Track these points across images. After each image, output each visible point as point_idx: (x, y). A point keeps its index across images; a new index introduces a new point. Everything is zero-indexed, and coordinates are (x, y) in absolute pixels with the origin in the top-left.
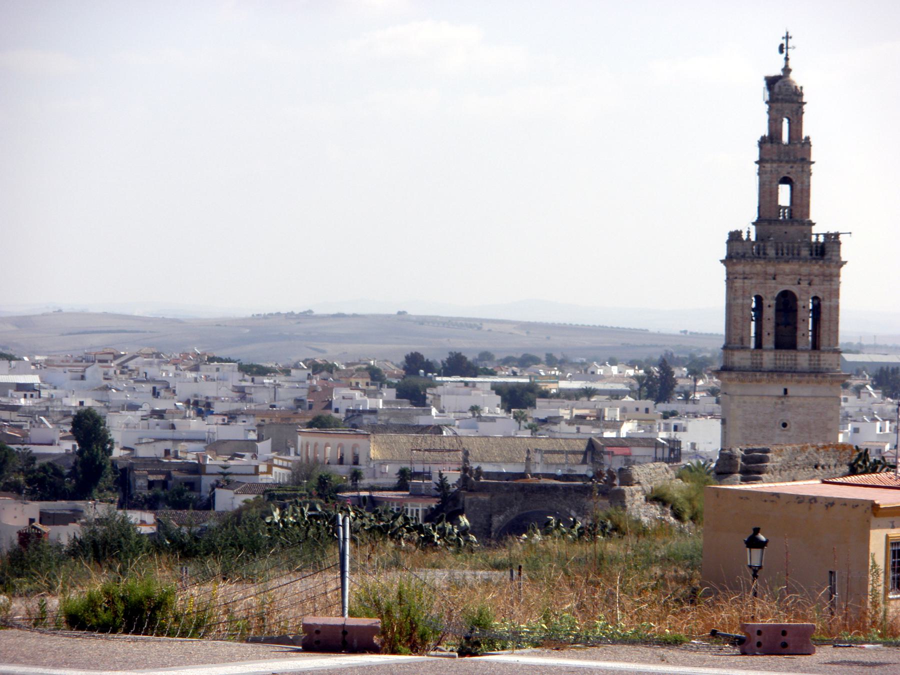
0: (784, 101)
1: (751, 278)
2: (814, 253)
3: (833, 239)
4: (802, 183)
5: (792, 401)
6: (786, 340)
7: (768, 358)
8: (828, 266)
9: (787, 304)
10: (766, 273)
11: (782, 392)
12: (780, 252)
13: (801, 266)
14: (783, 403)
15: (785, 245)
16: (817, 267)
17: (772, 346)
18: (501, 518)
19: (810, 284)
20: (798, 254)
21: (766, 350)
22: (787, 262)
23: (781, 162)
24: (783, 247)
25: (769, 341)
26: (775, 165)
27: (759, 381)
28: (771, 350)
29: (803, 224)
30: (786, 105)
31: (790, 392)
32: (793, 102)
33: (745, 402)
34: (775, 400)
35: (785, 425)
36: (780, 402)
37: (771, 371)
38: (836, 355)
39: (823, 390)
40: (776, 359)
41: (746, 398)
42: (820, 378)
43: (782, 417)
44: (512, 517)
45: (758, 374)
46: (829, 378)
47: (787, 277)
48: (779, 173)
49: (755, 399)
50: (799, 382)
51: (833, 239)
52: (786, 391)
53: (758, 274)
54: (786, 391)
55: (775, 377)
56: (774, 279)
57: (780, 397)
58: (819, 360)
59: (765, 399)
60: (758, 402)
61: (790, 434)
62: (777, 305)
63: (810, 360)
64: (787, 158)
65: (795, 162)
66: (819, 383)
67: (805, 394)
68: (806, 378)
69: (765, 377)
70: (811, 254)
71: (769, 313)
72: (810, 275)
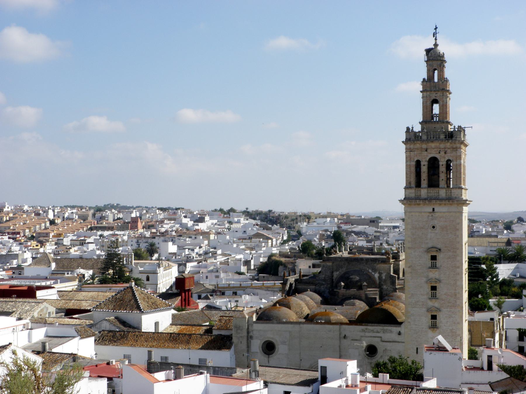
1: (414, 151)
2: (447, 137)
4: (443, 101)
5: (437, 214)
6: (433, 183)
7: (424, 192)
8: (455, 143)
9: (433, 163)
10: (422, 148)
11: (431, 210)
12: (429, 137)
13: (440, 144)
14: (432, 216)
15: (432, 133)
16: (449, 144)
17: (426, 186)
18: (338, 273)
19: (445, 153)
20: (439, 138)
21: (423, 188)
22: (432, 142)
23: (431, 91)
24: (430, 134)
25: (424, 183)
26: (428, 93)
27: (419, 204)
28: (425, 188)
29: (443, 122)
30: (434, 62)
31: (436, 210)
32: (438, 60)
33: (412, 216)
34: (428, 214)
35: (434, 227)
36: (430, 215)
37: (425, 199)
38: (460, 190)
40: (428, 193)
41: (413, 213)
42: (451, 202)
43: (432, 223)
44: (343, 273)
45: (418, 201)
46: (456, 202)
47: (433, 150)
48: (430, 97)
49: (417, 214)
50: (440, 205)
51: (461, 130)
52: (433, 209)
53: (418, 149)
54: (433, 209)
55: (427, 202)
56: (426, 151)
57: (430, 213)
58: (451, 193)
59: (423, 214)
60: (419, 216)
61: (436, 232)
62: (428, 164)
63: (446, 193)
64: (435, 89)
65: (438, 91)
66: (451, 204)
67: (444, 211)
68: (444, 202)
69: (421, 202)
70: (446, 138)
71: (424, 169)
72: (445, 148)
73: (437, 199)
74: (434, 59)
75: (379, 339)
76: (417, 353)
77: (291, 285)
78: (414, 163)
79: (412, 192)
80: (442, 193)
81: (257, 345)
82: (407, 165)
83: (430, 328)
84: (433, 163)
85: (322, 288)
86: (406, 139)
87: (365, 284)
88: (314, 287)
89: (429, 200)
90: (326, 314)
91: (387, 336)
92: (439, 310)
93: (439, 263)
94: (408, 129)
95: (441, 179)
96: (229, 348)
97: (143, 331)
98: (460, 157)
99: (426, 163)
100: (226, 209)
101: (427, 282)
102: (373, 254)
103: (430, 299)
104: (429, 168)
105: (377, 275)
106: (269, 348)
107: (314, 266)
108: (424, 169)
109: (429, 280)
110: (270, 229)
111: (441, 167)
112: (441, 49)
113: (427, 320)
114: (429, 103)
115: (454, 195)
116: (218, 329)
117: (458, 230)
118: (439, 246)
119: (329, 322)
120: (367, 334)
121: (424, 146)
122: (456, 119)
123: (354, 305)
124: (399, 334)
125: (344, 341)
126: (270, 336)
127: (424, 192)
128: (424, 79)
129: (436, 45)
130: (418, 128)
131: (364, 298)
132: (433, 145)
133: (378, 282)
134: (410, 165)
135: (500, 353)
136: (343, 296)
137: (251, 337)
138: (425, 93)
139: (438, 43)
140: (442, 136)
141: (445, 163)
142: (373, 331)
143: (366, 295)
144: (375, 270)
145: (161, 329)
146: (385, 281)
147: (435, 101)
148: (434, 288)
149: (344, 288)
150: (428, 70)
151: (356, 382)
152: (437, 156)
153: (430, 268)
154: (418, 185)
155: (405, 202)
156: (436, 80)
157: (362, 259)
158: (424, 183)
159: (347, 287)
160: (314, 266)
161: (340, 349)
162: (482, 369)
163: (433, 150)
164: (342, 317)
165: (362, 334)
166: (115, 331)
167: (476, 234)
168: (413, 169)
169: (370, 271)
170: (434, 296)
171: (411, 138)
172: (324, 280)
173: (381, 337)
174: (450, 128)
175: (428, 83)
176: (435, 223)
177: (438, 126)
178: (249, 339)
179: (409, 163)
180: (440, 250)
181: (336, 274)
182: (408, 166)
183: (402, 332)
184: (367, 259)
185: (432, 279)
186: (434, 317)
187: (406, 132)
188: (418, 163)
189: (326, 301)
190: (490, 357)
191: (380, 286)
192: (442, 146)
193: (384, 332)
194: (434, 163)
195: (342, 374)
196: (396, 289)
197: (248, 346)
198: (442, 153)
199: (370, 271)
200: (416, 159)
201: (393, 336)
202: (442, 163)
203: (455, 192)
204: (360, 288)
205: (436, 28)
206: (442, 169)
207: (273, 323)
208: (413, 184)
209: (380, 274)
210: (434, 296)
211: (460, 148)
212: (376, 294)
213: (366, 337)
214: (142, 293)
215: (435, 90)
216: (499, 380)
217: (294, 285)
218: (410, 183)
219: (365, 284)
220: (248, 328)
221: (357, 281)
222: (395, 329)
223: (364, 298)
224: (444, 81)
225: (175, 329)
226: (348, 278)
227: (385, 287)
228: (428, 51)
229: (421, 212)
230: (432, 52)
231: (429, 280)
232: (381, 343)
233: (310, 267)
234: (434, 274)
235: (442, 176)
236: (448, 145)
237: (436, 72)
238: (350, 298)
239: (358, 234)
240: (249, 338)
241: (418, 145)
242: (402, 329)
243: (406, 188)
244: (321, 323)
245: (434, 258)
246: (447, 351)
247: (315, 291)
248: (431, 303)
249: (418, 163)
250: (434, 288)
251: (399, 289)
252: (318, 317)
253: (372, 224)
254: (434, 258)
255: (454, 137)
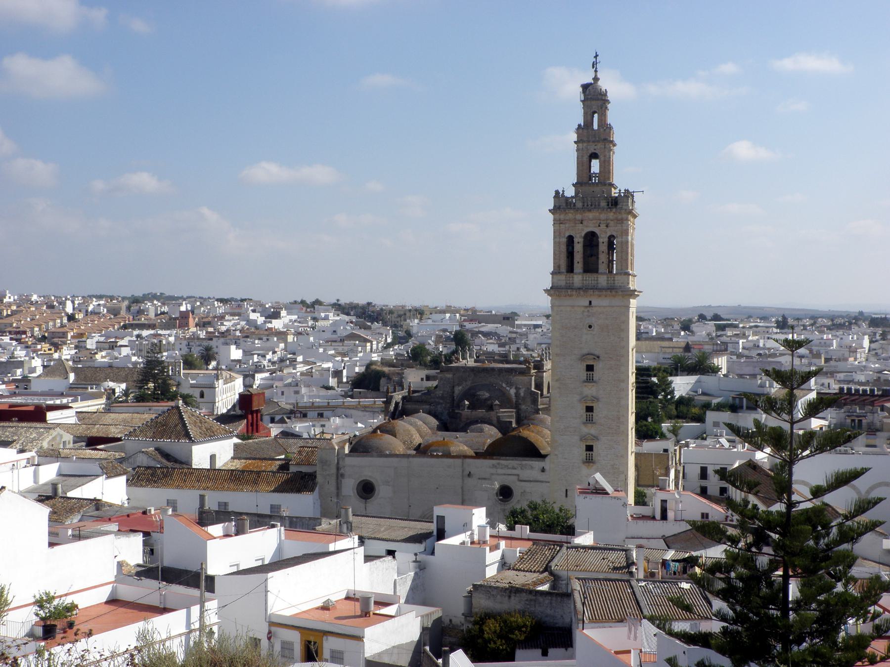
0: (592, 99)
3: (628, 195)
5: (595, 309)
6: (590, 267)
7: (578, 279)
9: (591, 239)
13: (600, 213)
17: (581, 271)
22: (590, 211)
23: (589, 142)
25: (578, 267)
26: (585, 144)
27: (571, 296)
28: (579, 274)
29: (605, 184)
30: (594, 102)
32: (598, 100)
34: (583, 309)
35: (590, 327)
37: (579, 289)
39: (617, 301)
47: (591, 222)
50: (600, 296)
51: (628, 195)
52: (590, 302)
53: (570, 220)
54: (590, 302)
57: (586, 307)
62: (584, 242)
65: (598, 142)
66: (614, 296)
71: (578, 248)
73: (595, 288)
74: (594, 98)
75: (515, 478)
76: (566, 496)
77: (397, 404)
78: (564, 240)
79: (562, 279)
80: (602, 280)
81: (349, 486)
82: (555, 243)
83: (584, 463)
84: (591, 239)
85: (439, 409)
86: (555, 206)
87: (497, 402)
88: (428, 407)
89: (584, 289)
90: (443, 443)
91: (526, 474)
92: (596, 438)
93: (597, 374)
94: (557, 192)
95: (600, 262)
96: (312, 490)
97: (194, 467)
98: (626, 233)
99: (581, 240)
100: (309, 301)
101: (580, 401)
102: (508, 362)
103: (584, 423)
104: (585, 246)
105: (513, 391)
106: (366, 490)
107: (428, 378)
108: (578, 248)
109: (583, 399)
110: (369, 328)
111: (601, 245)
112: (603, 84)
113: (580, 452)
114: (586, 158)
115: (617, 283)
116: (297, 464)
117: (623, 330)
118: (597, 353)
119: (447, 455)
120: (500, 471)
121: (579, 217)
122: (621, 181)
123: (482, 431)
124: (543, 470)
125: (469, 482)
126: (368, 474)
127: (578, 279)
128: (580, 125)
129: (596, 79)
130: (570, 192)
131: (495, 422)
132: (590, 215)
133: (514, 400)
134: (559, 243)
135: (677, 496)
136: (468, 419)
137: (342, 476)
138: (580, 145)
139: (599, 76)
140: (603, 204)
141: (606, 240)
142: (507, 467)
143: (498, 418)
144: (510, 384)
145: (219, 464)
146: (524, 398)
147: (594, 156)
148: (590, 409)
149: (469, 408)
150: (585, 114)
151: (485, 536)
152: (596, 230)
153: (585, 382)
154: (570, 269)
155: (552, 292)
156: (595, 127)
157: (493, 369)
158: (578, 267)
159: (472, 407)
160: (428, 378)
161: (463, 491)
162: (654, 518)
163: (591, 222)
164: (466, 448)
165: (493, 471)
166: (155, 468)
167: (644, 336)
168: (564, 248)
169: (504, 385)
170: (589, 420)
171: (562, 206)
172: (442, 398)
173: (518, 475)
174: (614, 193)
175: (585, 131)
176: (592, 320)
177: (597, 189)
178: (340, 478)
179: (557, 240)
180: (598, 357)
181: (458, 390)
182: (556, 244)
183: (547, 468)
184: (500, 370)
185: (587, 396)
186: (589, 448)
187: (555, 197)
188: (571, 239)
189: (444, 427)
190: (664, 502)
191: (517, 406)
192: (603, 216)
193: (522, 467)
194: (591, 239)
195: (466, 526)
196: (539, 410)
197: (338, 488)
198: (603, 226)
199: (504, 385)
200: (567, 235)
201: (535, 474)
202: (603, 240)
203: (619, 279)
204: (491, 408)
205: (596, 56)
206: (603, 247)
207: (372, 456)
208: (563, 268)
209: (517, 389)
210: (589, 420)
211: (627, 220)
212: (511, 417)
213: (498, 474)
214: (193, 415)
215: (595, 141)
216: (676, 533)
217: (400, 404)
218: (559, 267)
219: (497, 402)
220: (338, 463)
221: (486, 400)
222: (537, 464)
223: (495, 422)
224: (606, 128)
225: (238, 465)
226: (474, 395)
227: (523, 407)
228: (585, 87)
229: (573, 306)
230: (590, 88)
231: (583, 399)
232: (518, 483)
233: (422, 379)
234: (590, 390)
235: (603, 258)
236: (611, 215)
237: (596, 115)
238: (476, 422)
239: (487, 335)
240: (339, 476)
241: (570, 215)
242: (546, 463)
243: (553, 274)
244: (437, 456)
245: (590, 368)
246: (607, 494)
247: (430, 413)
248: (585, 430)
249: (571, 239)
250: (590, 409)
251: (543, 409)
252: (433, 448)
253: (506, 321)
254: (590, 368)
255: (619, 205)
